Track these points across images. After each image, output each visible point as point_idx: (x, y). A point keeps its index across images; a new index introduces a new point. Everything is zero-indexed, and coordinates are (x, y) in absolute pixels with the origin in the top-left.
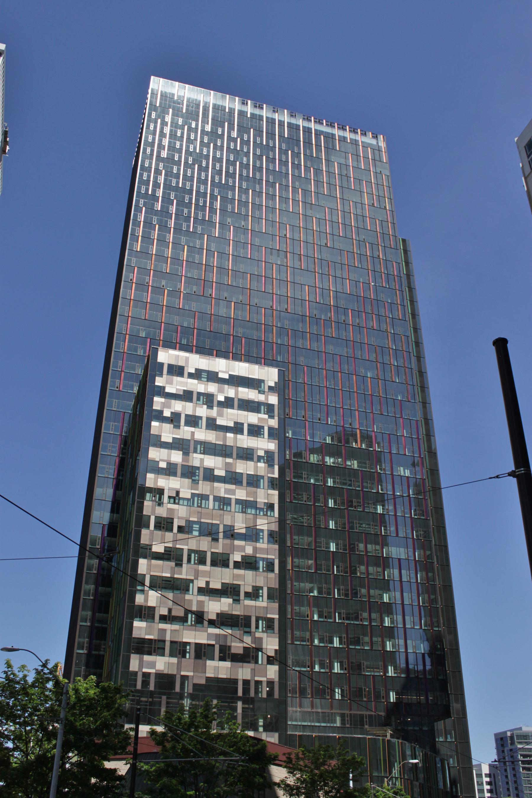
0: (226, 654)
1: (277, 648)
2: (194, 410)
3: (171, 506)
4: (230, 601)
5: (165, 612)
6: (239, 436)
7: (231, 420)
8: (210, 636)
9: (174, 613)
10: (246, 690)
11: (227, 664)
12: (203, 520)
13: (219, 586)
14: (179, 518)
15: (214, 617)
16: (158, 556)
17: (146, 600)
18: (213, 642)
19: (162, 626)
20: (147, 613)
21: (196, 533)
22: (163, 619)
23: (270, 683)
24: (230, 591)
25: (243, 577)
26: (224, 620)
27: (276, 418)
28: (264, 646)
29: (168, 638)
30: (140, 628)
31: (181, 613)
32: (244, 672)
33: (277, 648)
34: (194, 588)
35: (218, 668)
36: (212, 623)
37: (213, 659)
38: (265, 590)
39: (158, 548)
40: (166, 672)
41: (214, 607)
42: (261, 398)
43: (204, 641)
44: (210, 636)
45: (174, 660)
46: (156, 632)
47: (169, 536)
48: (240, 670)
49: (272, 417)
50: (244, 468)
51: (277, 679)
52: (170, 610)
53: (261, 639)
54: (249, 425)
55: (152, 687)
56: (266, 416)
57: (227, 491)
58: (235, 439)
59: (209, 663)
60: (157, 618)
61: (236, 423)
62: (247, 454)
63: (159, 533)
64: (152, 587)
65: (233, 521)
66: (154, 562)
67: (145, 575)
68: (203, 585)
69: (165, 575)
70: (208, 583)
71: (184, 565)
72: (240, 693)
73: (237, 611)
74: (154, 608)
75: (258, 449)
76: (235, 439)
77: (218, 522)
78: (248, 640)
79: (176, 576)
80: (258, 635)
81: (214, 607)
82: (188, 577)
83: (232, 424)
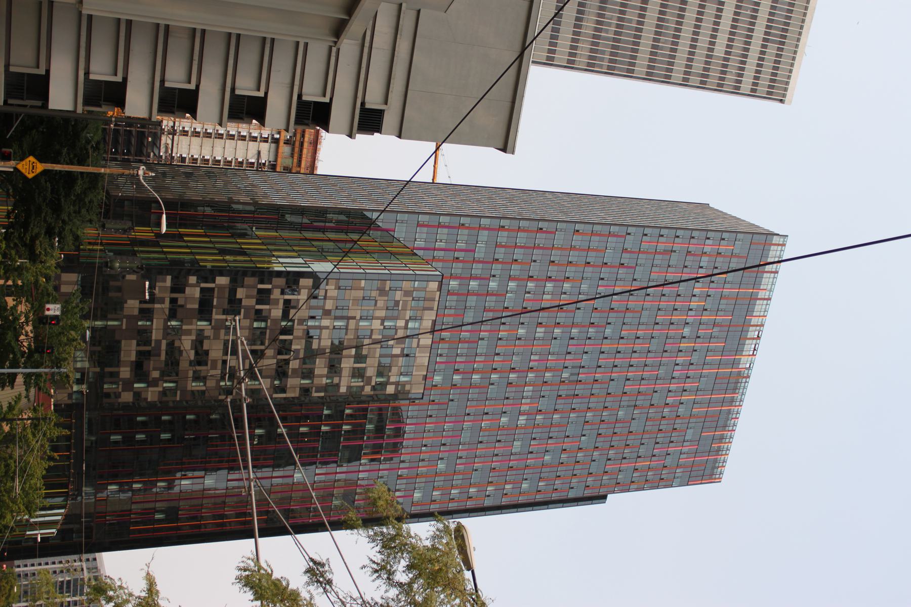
0: (143, 356)
1: (149, 400)
2: (377, 318)
3: (281, 302)
4: (192, 358)
5: (180, 302)
6: (352, 360)
7: (369, 352)
8: (158, 342)
9: (179, 310)
10: (112, 374)
11: (133, 357)
12: (268, 331)
13: (205, 347)
14: (270, 310)
15: (177, 344)
16: (233, 292)
17: (193, 286)
18: (153, 345)
19: (167, 301)
20: (178, 288)
21: (256, 325)
22: (173, 301)
23: (118, 395)
24: (202, 357)
25: (214, 367)
26: (173, 352)
27: (372, 393)
28: (150, 389)
29: (157, 306)
30: (165, 281)
31: (179, 315)
32: (125, 372)
33: (149, 400)
34: (202, 324)
35: (130, 350)
36: (171, 345)
37: (138, 345)
38: (204, 388)
39: (241, 293)
40: (125, 305)
41: (186, 343)
42: (393, 379)
43: (154, 338)
44: (158, 342)
45: (136, 312)
46: (161, 295)
47: (252, 302)
48: (128, 369)
49: (373, 388)
50: (320, 367)
51: (120, 400)
52: (182, 306)
53: (157, 386)
54: (365, 369)
55: (111, 294)
56: (373, 384)
57: (297, 351)
58: (349, 356)
59: (134, 342)
60: (175, 295)
61: (366, 357)
62: (334, 368)
63: (255, 292)
64: (203, 290)
65: (269, 358)
66: (227, 291)
67: (214, 282)
68: (206, 333)
69: (215, 300)
70: (208, 338)
71: (224, 317)
72: (107, 369)
73: (184, 365)
74: (184, 292)
75: (340, 377)
76: (349, 356)
77: (267, 344)
78: (155, 374)
79: (214, 310)
80: (160, 382)
81: (186, 343)
82: (213, 321)
83: (365, 352)
